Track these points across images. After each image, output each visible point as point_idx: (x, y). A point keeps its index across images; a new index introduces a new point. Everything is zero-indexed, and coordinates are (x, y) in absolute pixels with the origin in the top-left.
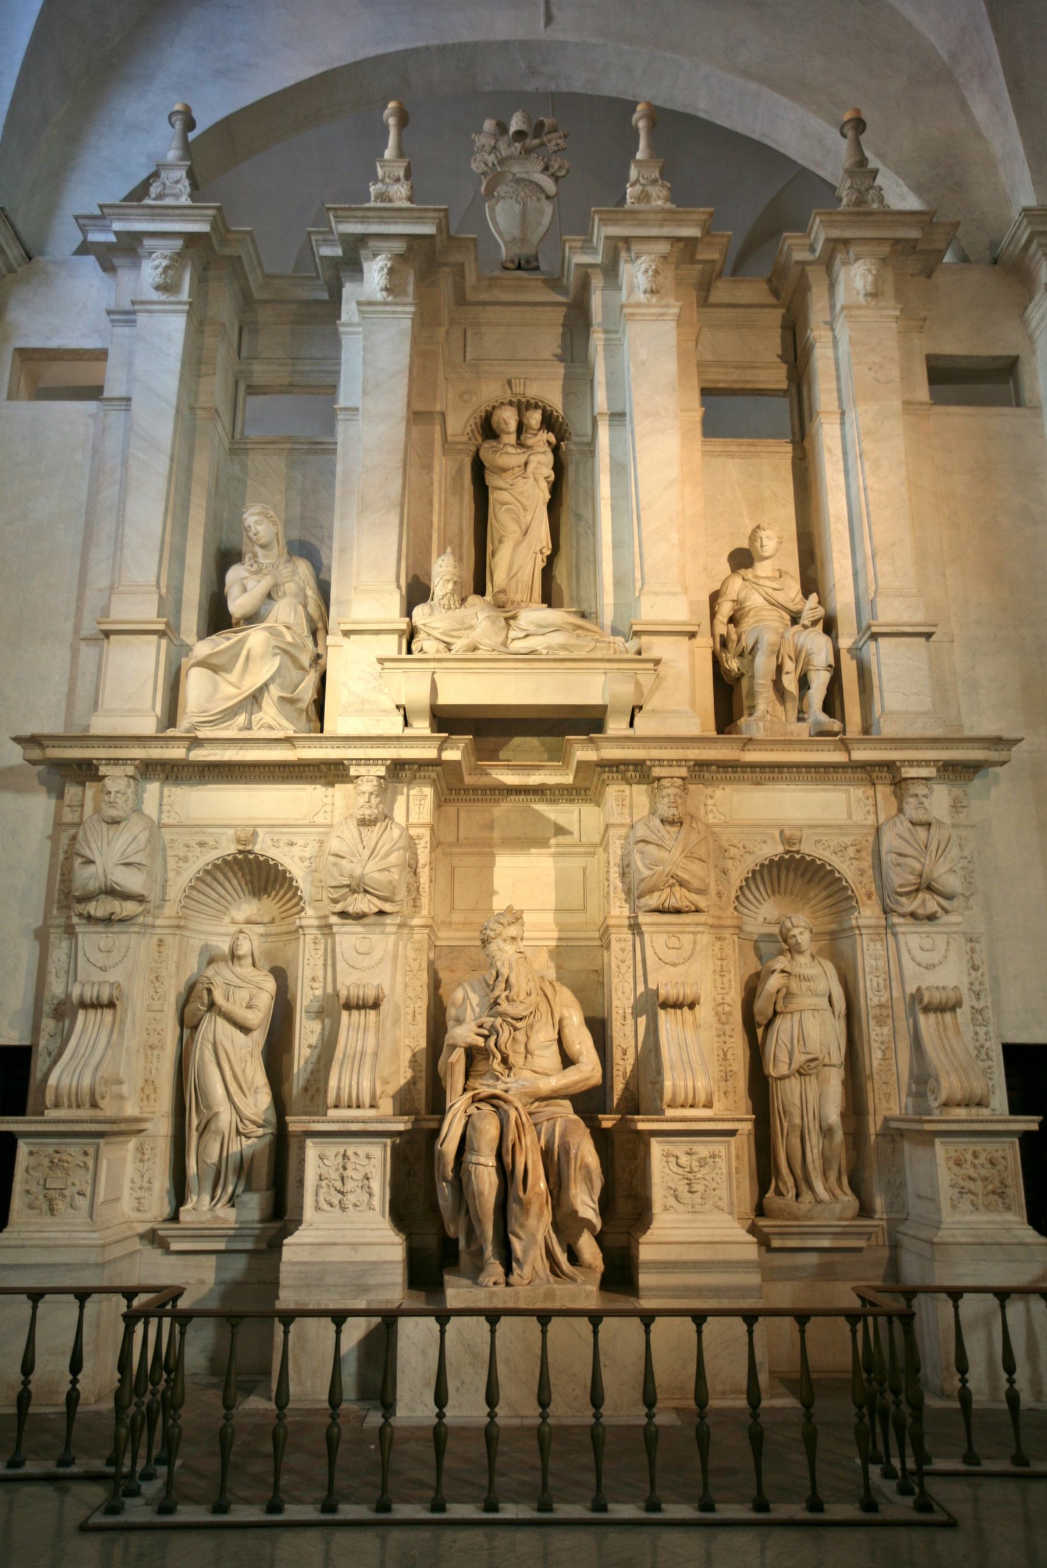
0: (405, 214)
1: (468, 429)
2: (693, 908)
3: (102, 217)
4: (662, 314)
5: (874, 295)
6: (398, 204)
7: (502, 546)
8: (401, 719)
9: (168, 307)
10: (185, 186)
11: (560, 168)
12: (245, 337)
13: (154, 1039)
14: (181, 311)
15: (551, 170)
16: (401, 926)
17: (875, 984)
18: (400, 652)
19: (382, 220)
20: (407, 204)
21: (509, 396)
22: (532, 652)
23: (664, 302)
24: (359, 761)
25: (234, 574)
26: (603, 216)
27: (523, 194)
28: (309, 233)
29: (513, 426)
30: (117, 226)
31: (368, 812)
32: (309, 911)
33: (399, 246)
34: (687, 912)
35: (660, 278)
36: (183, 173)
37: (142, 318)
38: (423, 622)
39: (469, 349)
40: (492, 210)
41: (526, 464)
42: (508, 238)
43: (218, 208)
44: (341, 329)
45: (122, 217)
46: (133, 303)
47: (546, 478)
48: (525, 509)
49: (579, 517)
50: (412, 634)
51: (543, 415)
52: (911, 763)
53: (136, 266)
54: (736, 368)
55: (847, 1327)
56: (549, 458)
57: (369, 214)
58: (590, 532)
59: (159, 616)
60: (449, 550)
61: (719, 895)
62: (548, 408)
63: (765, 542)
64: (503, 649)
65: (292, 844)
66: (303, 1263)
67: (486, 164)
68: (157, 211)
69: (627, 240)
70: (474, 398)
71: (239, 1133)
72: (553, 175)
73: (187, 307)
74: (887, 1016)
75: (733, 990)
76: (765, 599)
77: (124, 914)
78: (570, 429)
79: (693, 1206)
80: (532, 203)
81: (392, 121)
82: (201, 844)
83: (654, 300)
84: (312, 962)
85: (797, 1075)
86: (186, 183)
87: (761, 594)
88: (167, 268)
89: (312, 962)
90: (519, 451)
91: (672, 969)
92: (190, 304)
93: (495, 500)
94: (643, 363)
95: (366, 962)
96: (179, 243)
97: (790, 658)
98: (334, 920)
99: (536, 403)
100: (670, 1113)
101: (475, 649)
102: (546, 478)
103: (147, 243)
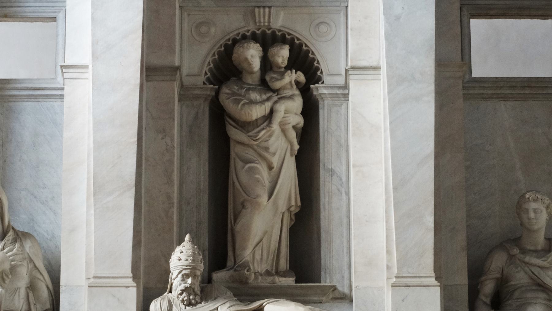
1: (206, 69)
7: (244, 211)
21: (252, 27)
29: (256, 64)
41: (272, 112)
47: (294, 127)
48: (270, 168)
49: (332, 172)
51: (290, 50)
58: (343, 190)
60: (187, 237)
62: (297, 42)
63: (532, 215)
70: (213, 30)
76: (532, 278)
78: (323, 66)
87: (526, 273)
90: (264, 97)
93: (237, 155)
94: (398, 18)
99: (283, 36)
102: (294, 127)
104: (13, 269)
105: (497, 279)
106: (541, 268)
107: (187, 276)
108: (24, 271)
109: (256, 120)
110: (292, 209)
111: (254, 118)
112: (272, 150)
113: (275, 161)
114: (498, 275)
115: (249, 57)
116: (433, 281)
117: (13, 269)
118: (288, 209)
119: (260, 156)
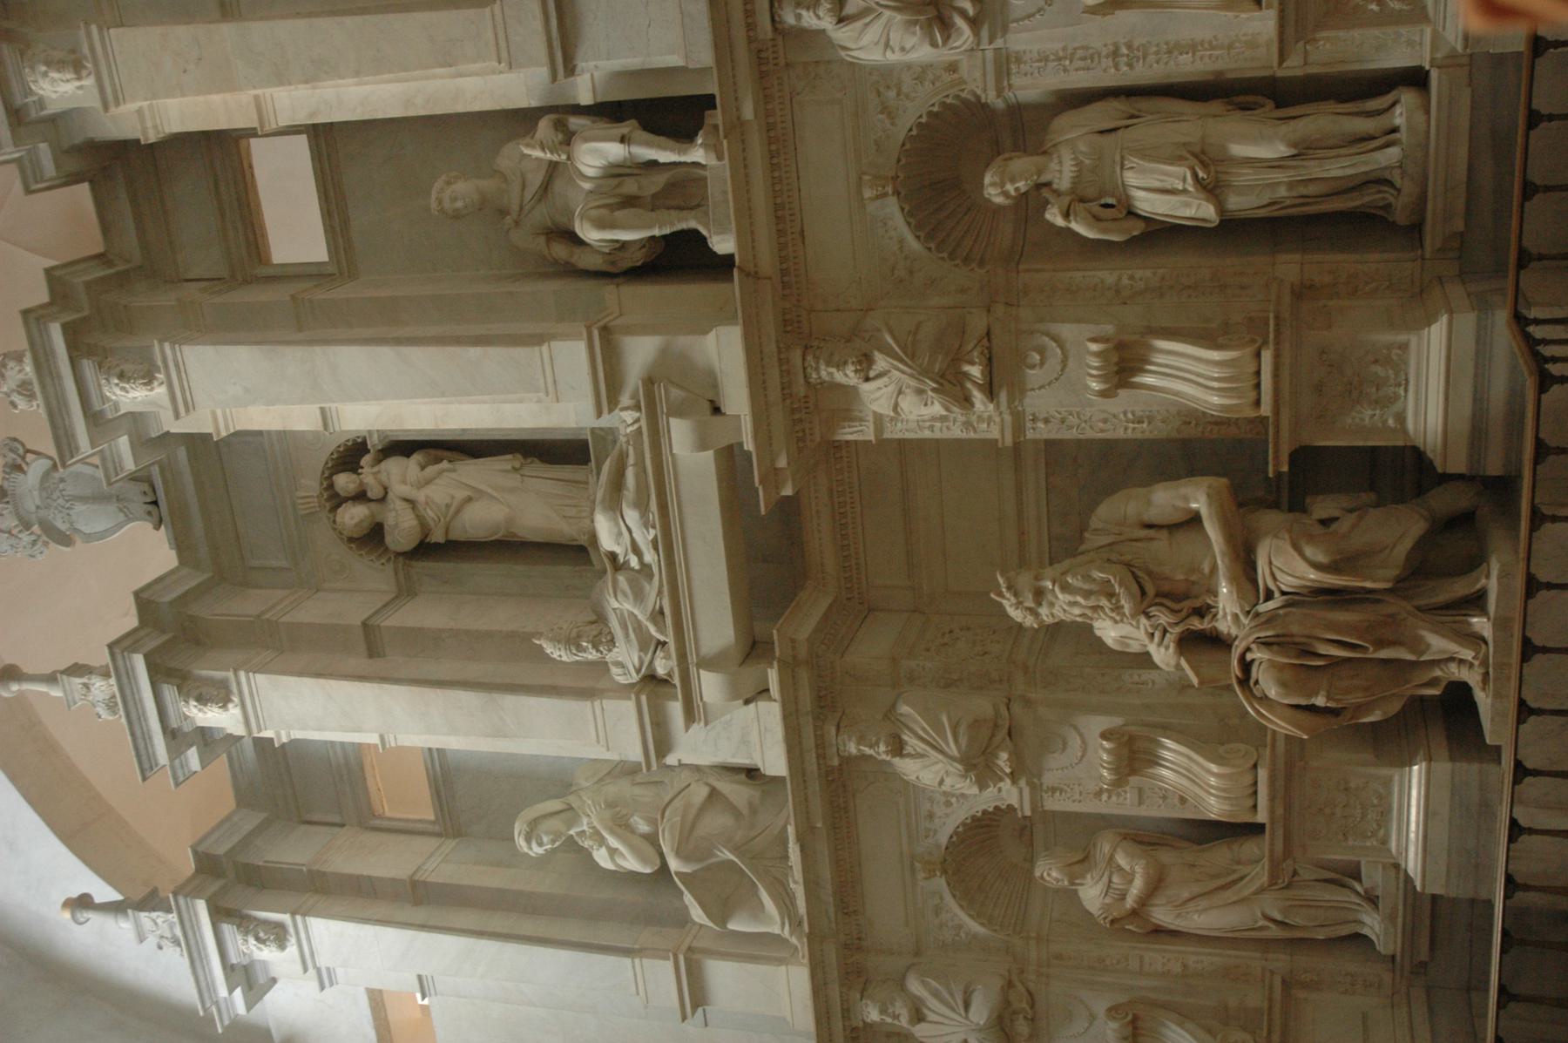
0: (128, 692)
2: (985, 341)
3: (217, 1004)
4: (177, 366)
5: (78, 67)
6: (115, 689)
8: (762, 705)
9: (303, 935)
10: (159, 916)
11: (11, 450)
12: (316, 817)
13: (1177, 968)
14: (305, 923)
15: (19, 461)
16: (1028, 703)
17: (1081, 64)
18: (676, 699)
19: (142, 716)
20: (113, 681)
22: (656, 549)
23: (160, 363)
24: (821, 757)
25: (602, 858)
26: (67, 454)
27: (60, 501)
28: (177, 784)
30: (223, 992)
31: (882, 748)
32: (1015, 802)
33: (169, 692)
34: (989, 349)
35: (127, 367)
36: (143, 914)
37: (323, 962)
38: (634, 674)
39: (275, 563)
40: (89, 538)
41: (406, 500)
42: (121, 517)
43: (175, 894)
44: (285, 740)
45: (211, 987)
46: (306, 970)
48: (469, 499)
50: (651, 679)
52: (751, 27)
53: (264, 962)
54: (223, 215)
55: (1556, 389)
56: (395, 468)
57: (138, 733)
59: (666, 958)
61: (962, 291)
64: (656, 578)
65: (931, 816)
66: (1448, 872)
67: (34, 543)
68: (195, 955)
69: (95, 419)
71: (1288, 887)
72: (23, 458)
73: (298, 918)
74: (1129, 47)
75: (1100, 274)
77: (1024, 1005)
79: (1399, 385)
80: (70, 490)
81: (15, 687)
82: (937, 911)
83: (161, 376)
84: (1077, 797)
85: (1218, 191)
86: (154, 915)
88: (257, 939)
89: (1077, 797)
91: (1071, 364)
92: (293, 914)
95: (1075, 742)
96: (228, 929)
97: (618, 186)
98: (1022, 783)
100: (1266, 409)
101: (662, 612)
102: (423, 468)
103: (234, 960)
104: (610, 805)
105: (548, 241)
106: (524, 186)
107: (580, 648)
108: (612, 790)
109: (418, 517)
110: (517, 465)
111: (415, 522)
112: (448, 500)
113: (462, 494)
114: (542, 239)
115: (356, 520)
116: (545, 348)
117: (610, 805)
118: (515, 469)
119: (458, 512)
